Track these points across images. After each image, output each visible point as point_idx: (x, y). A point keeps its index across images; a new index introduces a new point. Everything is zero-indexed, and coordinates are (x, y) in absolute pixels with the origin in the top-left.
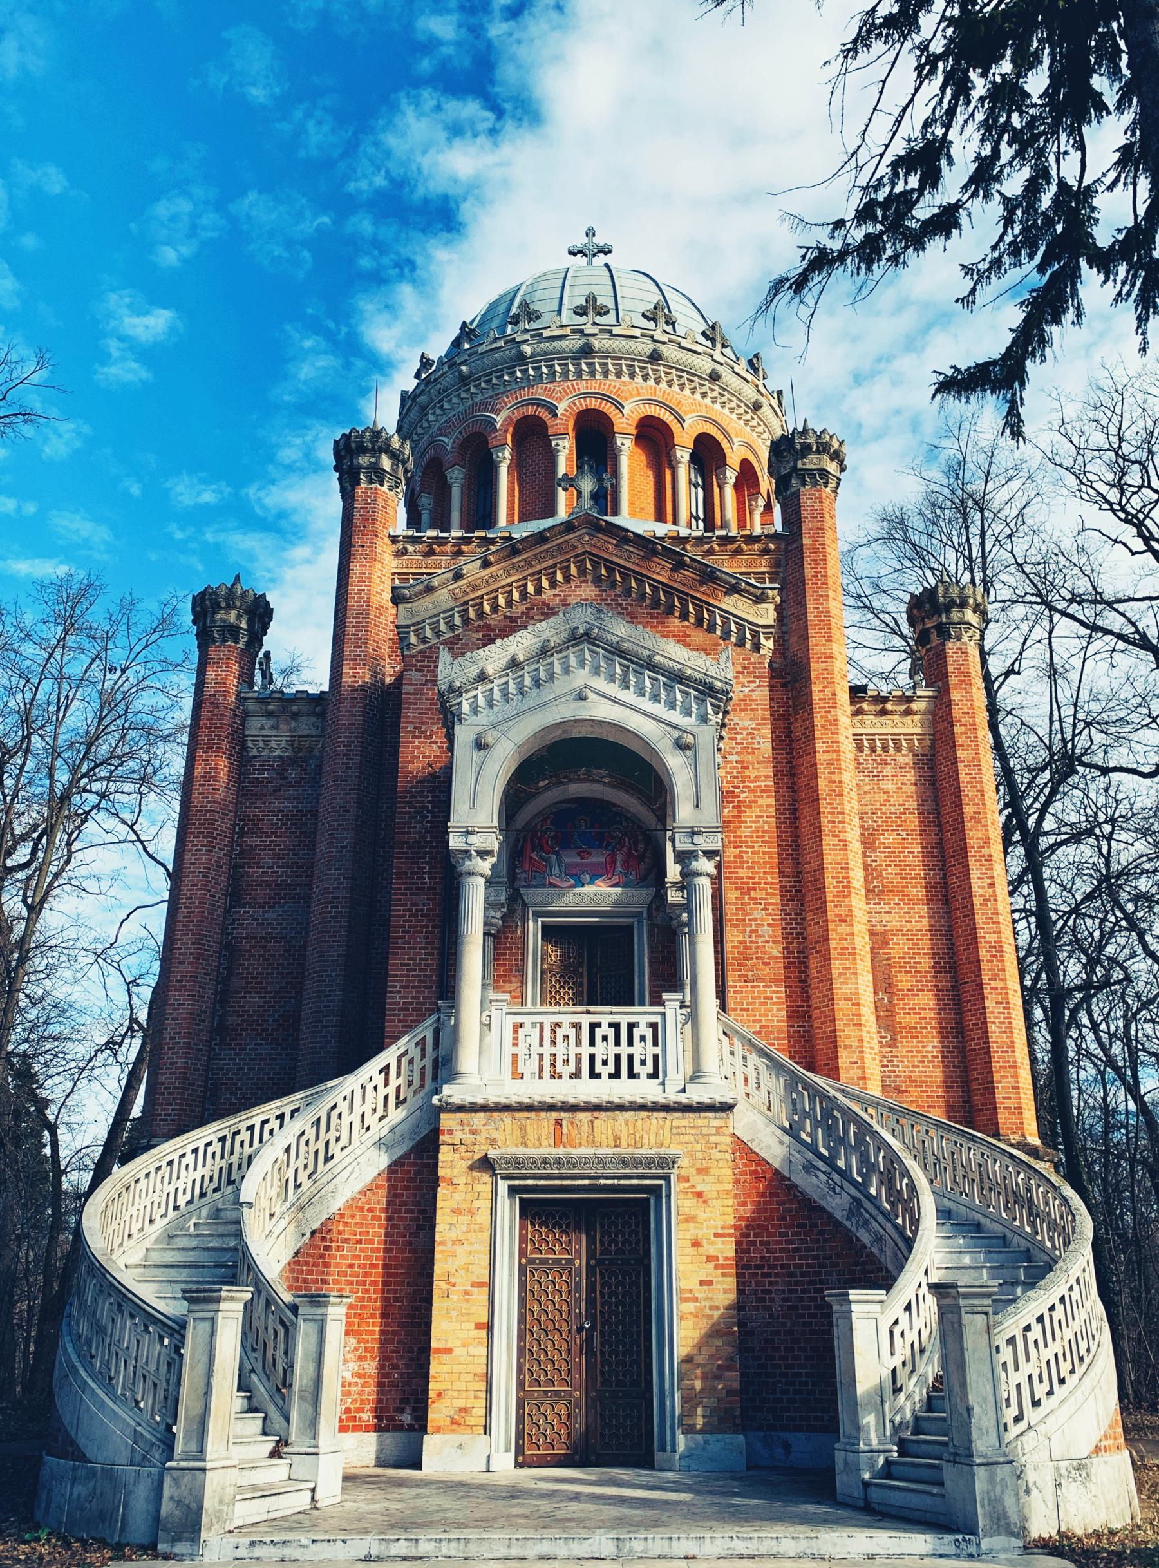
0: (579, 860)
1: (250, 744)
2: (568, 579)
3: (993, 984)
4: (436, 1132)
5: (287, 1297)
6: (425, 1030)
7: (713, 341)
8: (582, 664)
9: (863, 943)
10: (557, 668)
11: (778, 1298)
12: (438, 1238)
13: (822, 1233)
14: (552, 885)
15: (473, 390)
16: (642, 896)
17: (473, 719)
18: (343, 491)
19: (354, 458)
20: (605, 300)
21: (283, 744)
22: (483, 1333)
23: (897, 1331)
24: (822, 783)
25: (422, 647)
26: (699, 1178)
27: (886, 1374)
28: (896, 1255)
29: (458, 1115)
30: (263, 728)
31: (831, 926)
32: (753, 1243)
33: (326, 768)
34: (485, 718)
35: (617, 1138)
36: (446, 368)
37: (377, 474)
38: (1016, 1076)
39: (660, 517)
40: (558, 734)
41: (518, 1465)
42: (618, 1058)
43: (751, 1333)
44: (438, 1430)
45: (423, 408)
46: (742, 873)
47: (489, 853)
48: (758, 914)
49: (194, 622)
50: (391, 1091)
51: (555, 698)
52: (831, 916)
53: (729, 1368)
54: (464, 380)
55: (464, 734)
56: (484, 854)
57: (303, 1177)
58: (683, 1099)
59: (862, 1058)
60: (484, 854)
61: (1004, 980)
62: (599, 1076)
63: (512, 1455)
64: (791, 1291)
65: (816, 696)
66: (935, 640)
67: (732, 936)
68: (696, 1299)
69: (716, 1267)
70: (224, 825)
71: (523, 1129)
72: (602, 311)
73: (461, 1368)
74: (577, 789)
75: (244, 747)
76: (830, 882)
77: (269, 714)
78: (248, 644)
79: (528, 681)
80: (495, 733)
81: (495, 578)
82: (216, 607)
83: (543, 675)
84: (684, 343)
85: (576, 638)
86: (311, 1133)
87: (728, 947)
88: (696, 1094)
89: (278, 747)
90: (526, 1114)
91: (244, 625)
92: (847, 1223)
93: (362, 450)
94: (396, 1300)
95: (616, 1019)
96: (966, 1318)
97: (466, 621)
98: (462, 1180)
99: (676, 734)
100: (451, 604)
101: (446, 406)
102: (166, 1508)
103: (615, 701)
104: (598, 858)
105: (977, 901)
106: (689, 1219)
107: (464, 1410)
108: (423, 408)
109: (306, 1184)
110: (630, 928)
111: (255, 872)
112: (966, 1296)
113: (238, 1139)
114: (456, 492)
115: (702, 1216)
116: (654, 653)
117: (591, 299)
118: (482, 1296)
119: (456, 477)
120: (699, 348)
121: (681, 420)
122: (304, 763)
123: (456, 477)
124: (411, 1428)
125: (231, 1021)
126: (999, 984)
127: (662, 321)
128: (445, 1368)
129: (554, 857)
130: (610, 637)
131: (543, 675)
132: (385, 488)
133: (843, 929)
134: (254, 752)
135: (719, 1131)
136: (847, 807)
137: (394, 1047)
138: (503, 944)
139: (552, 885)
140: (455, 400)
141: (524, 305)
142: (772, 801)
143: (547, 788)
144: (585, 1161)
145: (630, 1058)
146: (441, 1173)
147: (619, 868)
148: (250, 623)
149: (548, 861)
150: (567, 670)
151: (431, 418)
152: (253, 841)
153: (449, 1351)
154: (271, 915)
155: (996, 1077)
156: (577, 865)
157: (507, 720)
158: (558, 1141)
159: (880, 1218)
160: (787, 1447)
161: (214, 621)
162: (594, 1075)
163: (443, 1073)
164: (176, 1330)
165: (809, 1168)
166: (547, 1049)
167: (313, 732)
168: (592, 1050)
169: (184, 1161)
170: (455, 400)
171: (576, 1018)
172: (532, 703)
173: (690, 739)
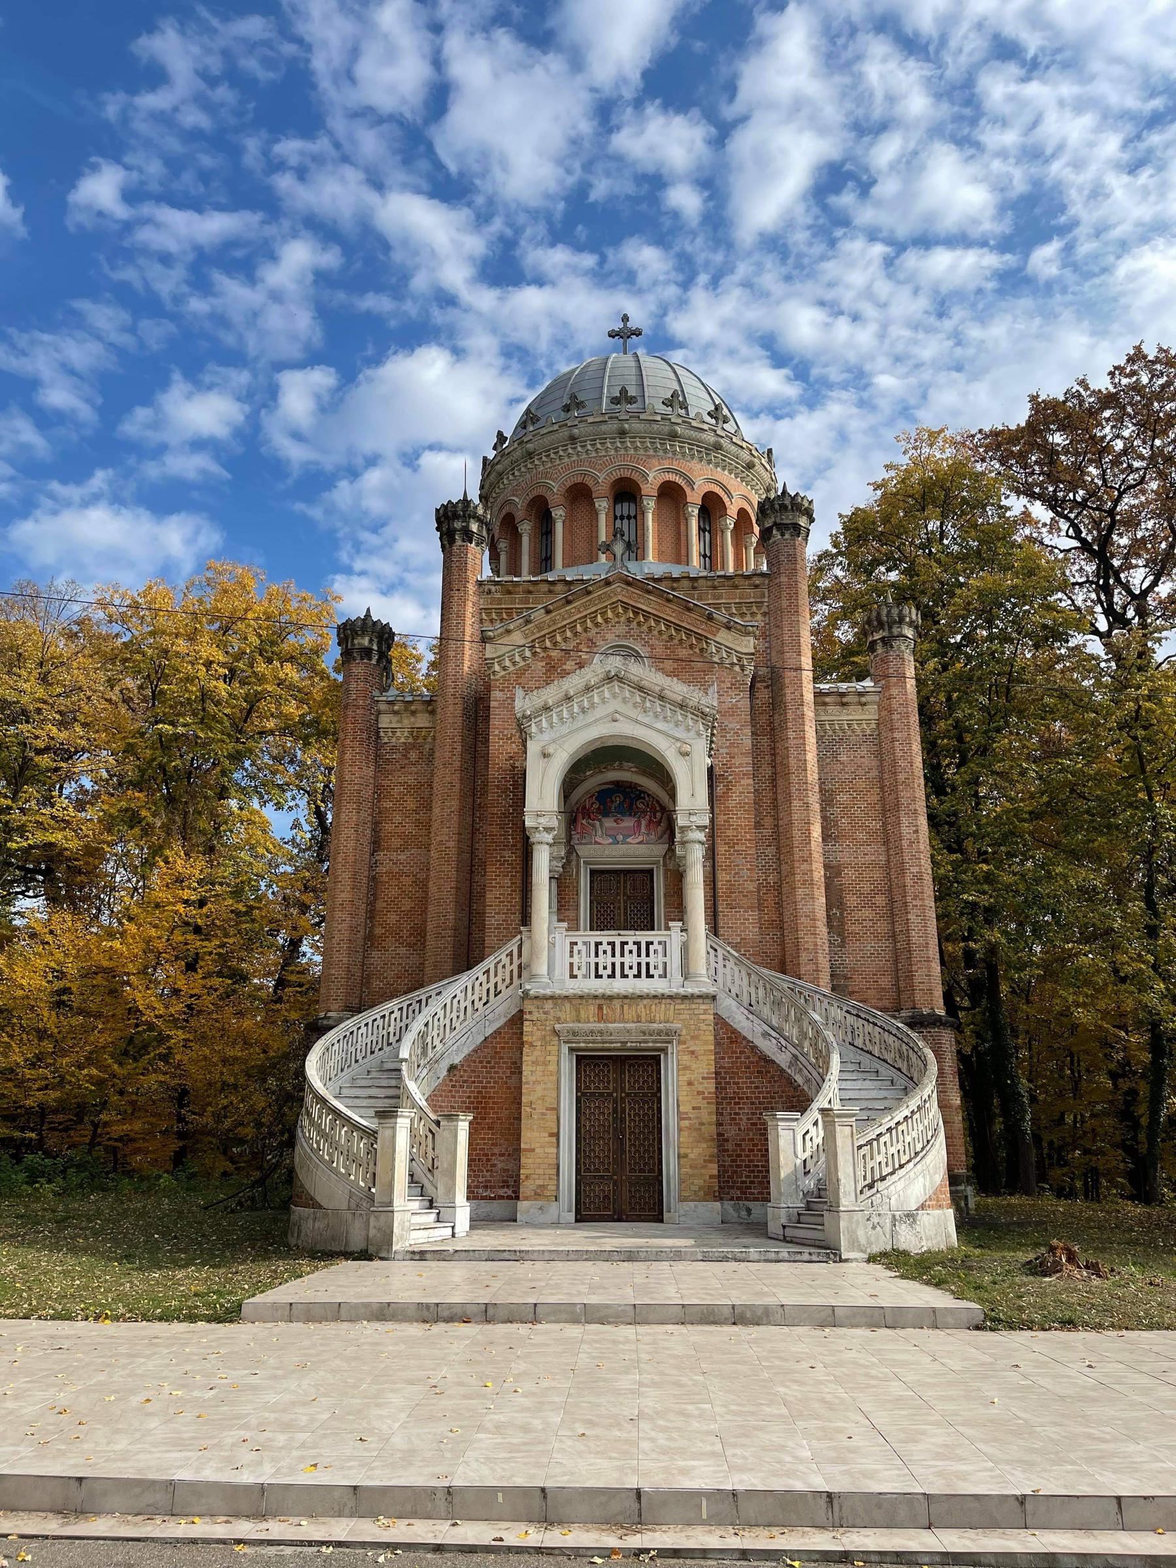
0: (615, 824)
1: (382, 734)
2: (606, 621)
3: (914, 903)
4: (521, 1011)
5: (433, 1117)
6: (513, 946)
7: (716, 419)
8: (614, 696)
9: (819, 873)
10: (596, 699)
11: (744, 1118)
12: (524, 1079)
14: (597, 843)
15: (537, 462)
16: (660, 849)
17: (539, 737)
18: (443, 546)
19: (451, 521)
20: (632, 392)
22: (554, 1140)
23: (808, 1137)
24: (792, 762)
25: (503, 673)
26: (692, 1043)
27: (799, 1162)
29: (535, 1002)
30: (391, 722)
31: (797, 865)
32: (729, 1083)
33: (437, 754)
34: (547, 737)
35: (639, 1016)
36: (516, 445)
37: (468, 536)
38: (929, 968)
39: (678, 562)
40: (598, 745)
41: (577, 1221)
42: (639, 964)
43: (727, 1140)
44: (526, 1199)
45: (500, 475)
46: (729, 833)
47: (552, 829)
48: (740, 860)
49: (339, 644)
50: (491, 985)
51: (596, 721)
52: (796, 857)
53: (710, 1162)
54: (530, 455)
55: (533, 748)
56: (548, 830)
57: (437, 1042)
58: (682, 991)
59: (816, 957)
60: (548, 830)
61: (923, 899)
62: (627, 976)
63: (573, 1214)
64: (753, 1114)
65: (789, 697)
66: (880, 649)
67: (722, 877)
68: (689, 1119)
69: (703, 1099)
70: (368, 792)
71: (578, 1011)
72: (631, 400)
73: (539, 1161)
74: (613, 775)
75: (378, 737)
76: (796, 833)
77: (395, 713)
78: (378, 661)
79: (576, 710)
80: (554, 745)
81: (554, 622)
82: (355, 634)
83: (586, 704)
84: (694, 424)
85: (609, 679)
86: (441, 1014)
87: (719, 885)
88: (690, 989)
89: (402, 737)
90: (579, 1001)
91: (375, 647)
92: (789, 1071)
93: (456, 516)
94: (498, 1119)
95: (638, 939)
96: (838, 1128)
97: (534, 654)
98: (539, 1043)
99: (678, 744)
101: (517, 473)
102: (372, 1232)
103: (637, 721)
104: (629, 822)
105: (905, 843)
106: (686, 1068)
107: (543, 1187)
108: (500, 475)
109: (439, 1047)
110: (651, 872)
111: (388, 827)
112: (839, 1116)
113: (393, 1016)
114: (525, 540)
115: (694, 1066)
116: (663, 690)
117: (624, 391)
118: (551, 1116)
119: (526, 529)
120: (706, 427)
121: (691, 484)
122: (422, 748)
123: (526, 529)
124: (509, 1198)
125: (378, 931)
126: (919, 903)
127: (677, 406)
128: (530, 1161)
129: (597, 823)
130: (632, 677)
131: (586, 704)
132: (473, 545)
133: (805, 866)
134: (386, 740)
135: (705, 1012)
136: (810, 779)
137: (492, 958)
138: (563, 884)
139: (597, 843)
140: (523, 469)
141: (573, 397)
142: (751, 781)
143: (591, 776)
144: (619, 1031)
145: (648, 964)
146: (525, 1039)
147: (643, 830)
148: (379, 644)
149: (594, 826)
150: (603, 700)
151: (506, 482)
152: (387, 804)
153: (533, 1150)
154: (402, 857)
155: (914, 968)
156: (613, 828)
157: (562, 737)
158: (601, 1018)
159: (810, 1067)
160: (749, 1211)
161: (353, 644)
162: (624, 976)
163: (525, 974)
164: (372, 1135)
165: (765, 1035)
166: (593, 960)
167: (427, 725)
168: (622, 960)
169: (360, 1031)
170: (523, 469)
171: (611, 939)
172: (580, 724)
173: (687, 748)
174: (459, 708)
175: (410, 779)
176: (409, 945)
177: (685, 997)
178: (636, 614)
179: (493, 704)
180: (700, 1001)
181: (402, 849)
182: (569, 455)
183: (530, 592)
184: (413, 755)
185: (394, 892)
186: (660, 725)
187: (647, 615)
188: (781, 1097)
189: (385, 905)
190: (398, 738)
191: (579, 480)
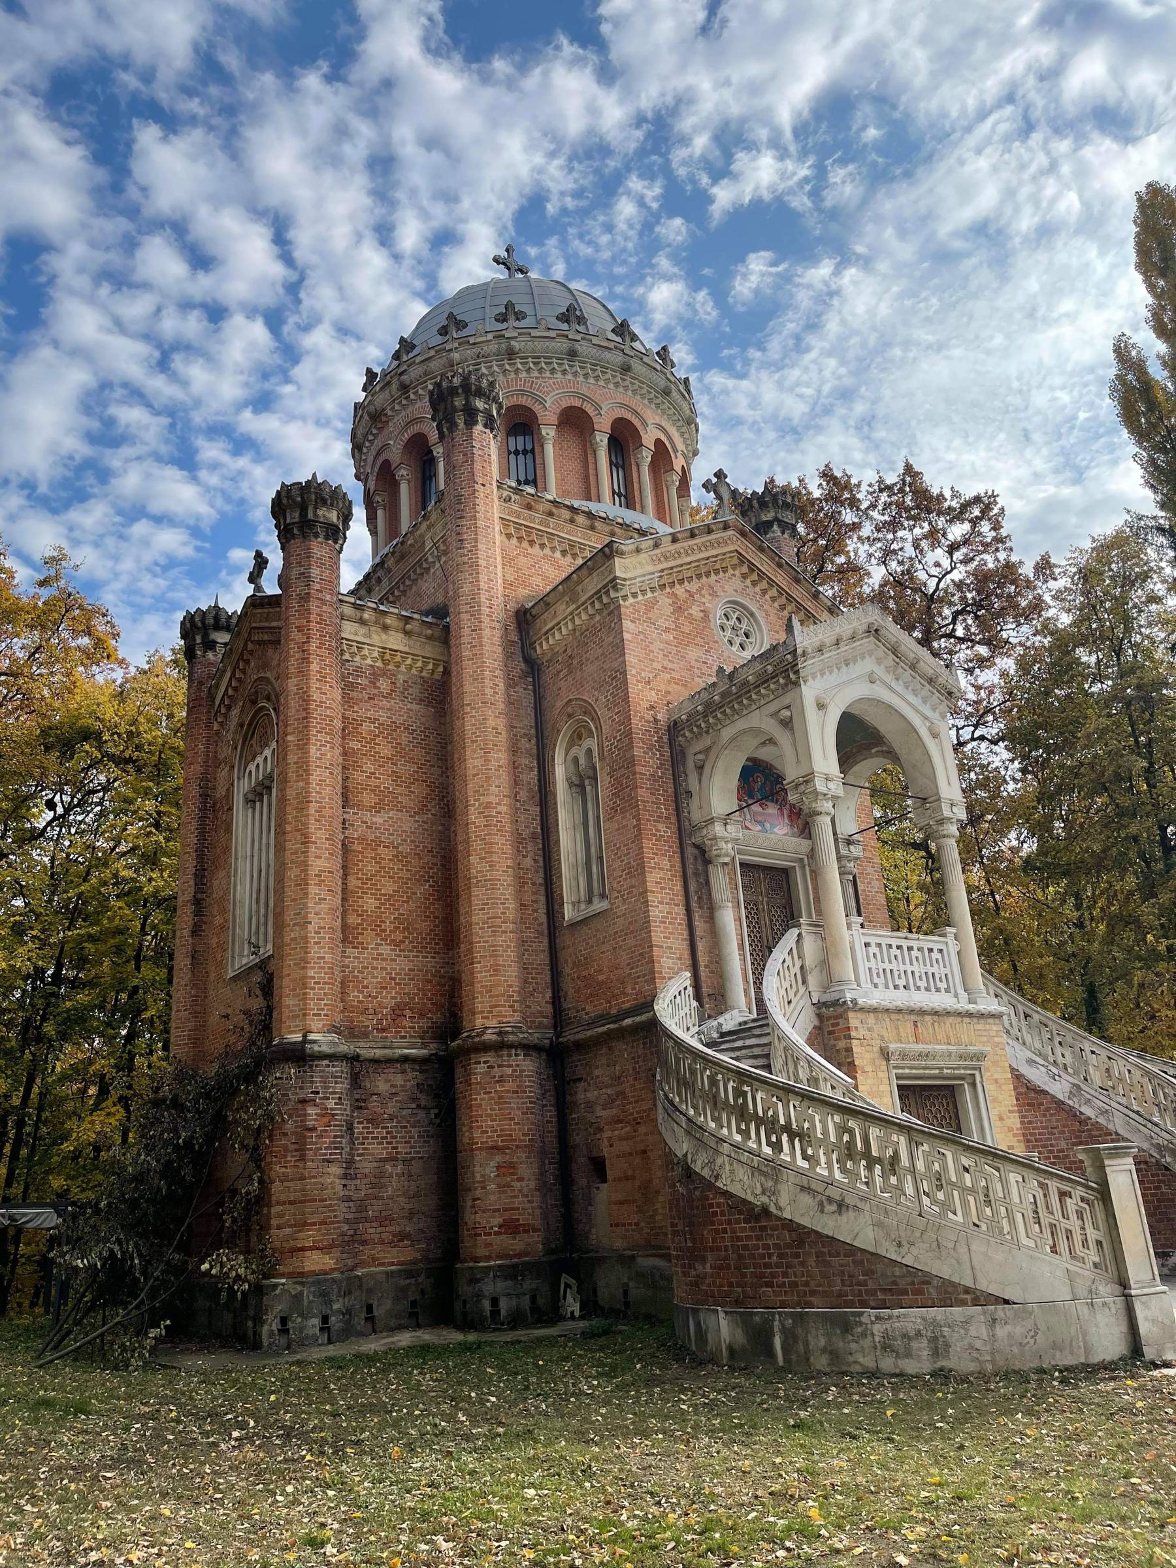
13: (1048, 1109)
21: (376, 654)
28: (1128, 1124)
35: (948, 1038)
71: (897, 1028)
77: (362, 622)
100: (650, 568)
154: (378, 820)
165: (1030, 1062)
167: (406, 649)
174: (498, 634)
175: (384, 717)
176: (394, 943)
177: (970, 1015)
178: (751, 570)
179: (626, 636)
180: (991, 1021)
181: (377, 808)
182: (564, 372)
183: (551, 514)
184: (384, 685)
185: (370, 868)
186: (911, 698)
187: (762, 575)
188: (1063, 1132)
189: (359, 883)
190: (364, 658)
191: (577, 403)
